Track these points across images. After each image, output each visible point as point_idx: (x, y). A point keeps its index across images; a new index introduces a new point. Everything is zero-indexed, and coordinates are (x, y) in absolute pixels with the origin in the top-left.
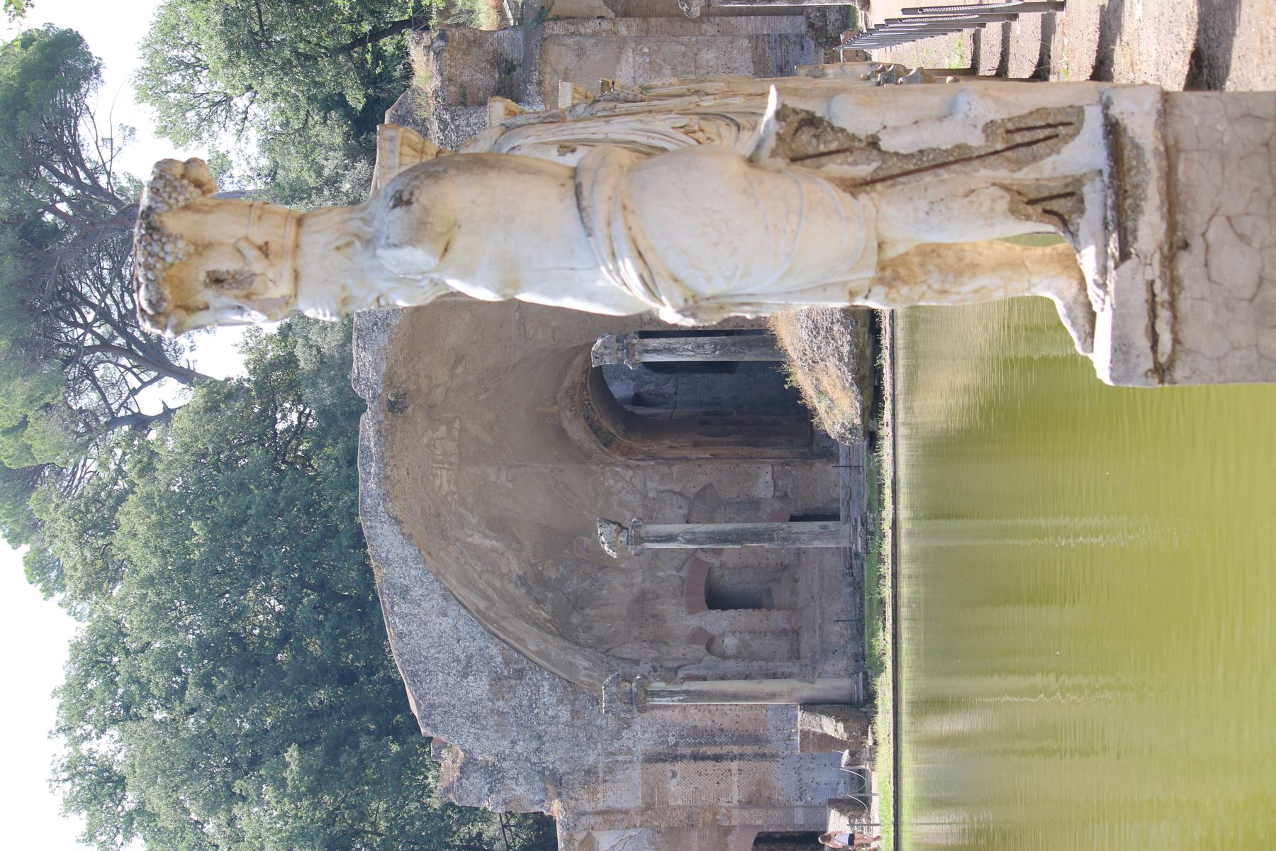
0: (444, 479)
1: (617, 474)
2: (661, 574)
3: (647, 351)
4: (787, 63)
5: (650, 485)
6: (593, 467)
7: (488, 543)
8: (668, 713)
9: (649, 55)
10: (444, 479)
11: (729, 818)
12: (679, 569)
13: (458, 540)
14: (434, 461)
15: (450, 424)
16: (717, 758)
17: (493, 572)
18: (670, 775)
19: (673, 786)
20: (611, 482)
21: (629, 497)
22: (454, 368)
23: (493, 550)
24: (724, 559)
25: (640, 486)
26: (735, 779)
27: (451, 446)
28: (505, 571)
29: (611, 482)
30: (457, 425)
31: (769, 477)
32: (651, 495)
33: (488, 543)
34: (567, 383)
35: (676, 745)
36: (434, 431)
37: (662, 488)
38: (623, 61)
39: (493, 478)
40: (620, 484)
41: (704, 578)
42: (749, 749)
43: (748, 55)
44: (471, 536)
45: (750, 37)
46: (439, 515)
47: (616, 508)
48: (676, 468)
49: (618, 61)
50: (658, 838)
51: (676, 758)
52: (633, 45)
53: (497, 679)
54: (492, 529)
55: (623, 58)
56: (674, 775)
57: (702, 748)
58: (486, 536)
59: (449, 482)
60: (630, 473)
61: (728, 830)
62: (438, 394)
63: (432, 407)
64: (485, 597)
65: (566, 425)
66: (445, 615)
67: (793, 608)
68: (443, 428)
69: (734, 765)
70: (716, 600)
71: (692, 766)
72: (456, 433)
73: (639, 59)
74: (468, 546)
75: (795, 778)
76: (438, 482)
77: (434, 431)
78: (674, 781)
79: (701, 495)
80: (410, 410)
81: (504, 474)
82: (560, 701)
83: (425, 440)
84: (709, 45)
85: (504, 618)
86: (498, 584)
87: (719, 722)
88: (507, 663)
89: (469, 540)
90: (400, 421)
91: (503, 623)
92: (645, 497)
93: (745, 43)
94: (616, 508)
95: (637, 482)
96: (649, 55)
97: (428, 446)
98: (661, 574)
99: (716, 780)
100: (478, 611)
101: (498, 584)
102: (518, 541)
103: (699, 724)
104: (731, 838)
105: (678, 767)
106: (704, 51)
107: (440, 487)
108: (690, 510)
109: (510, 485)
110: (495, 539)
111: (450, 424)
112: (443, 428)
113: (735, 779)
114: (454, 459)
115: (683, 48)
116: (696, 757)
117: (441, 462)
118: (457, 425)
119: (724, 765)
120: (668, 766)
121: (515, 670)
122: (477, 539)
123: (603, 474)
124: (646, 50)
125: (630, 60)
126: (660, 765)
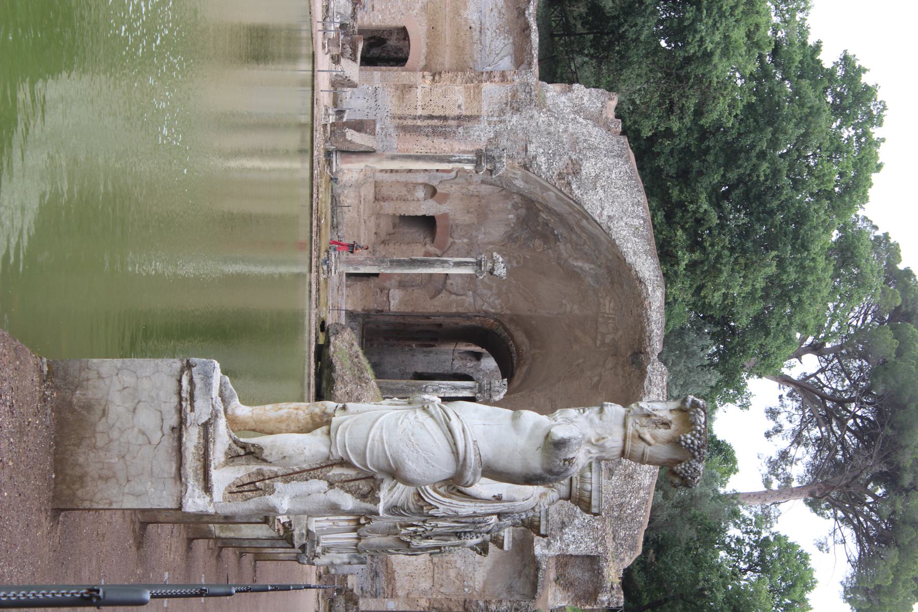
0: (607, 307)
1: (492, 308)
2: (465, 240)
3: (471, 388)
4: (372, 579)
5: (472, 300)
6: (509, 312)
7: (580, 264)
8: (462, 148)
9: (464, 586)
10: (607, 307)
11: (424, 77)
12: (453, 243)
13: (600, 266)
14: (614, 319)
15: (603, 343)
16: (431, 117)
17: (577, 244)
18: (463, 107)
19: (461, 100)
20: (497, 302)
21: (485, 291)
22: (599, 381)
23: (576, 259)
24: (423, 250)
25: (478, 298)
26: (419, 103)
27: (602, 329)
28: (569, 245)
29: (497, 302)
30: (598, 343)
31: (392, 302)
32: (471, 293)
33: (580, 264)
34: (524, 369)
35: (458, 126)
37: (464, 297)
38: (482, 583)
39: (575, 307)
40: (491, 300)
41: (437, 237)
42: (410, 122)
43: (398, 584)
44: (590, 269)
45: (397, 596)
46: (612, 283)
47: (494, 285)
48: (454, 310)
49: (485, 583)
50: (471, 65)
51: (459, 118)
52: (475, 593)
53: (576, 173)
54: (577, 273)
55: (481, 585)
56: (459, 106)
57: (441, 125)
58: (581, 268)
59: (604, 305)
60: (484, 308)
61: (425, 68)
62: (610, 363)
63: (615, 355)
64: (583, 229)
65: (526, 341)
66: (609, 217)
67: (378, 216)
68: (607, 341)
69: (419, 112)
70: (428, 223)
71: (447, 113)
72: (599, 337)
73: (471, 584)
74: (593, 263)
75: (379, 103)
76: (612, 305)
77: (614, 339)
78: (460, 102)
79: (439, 292)
80: (629, 353)
81: (568, 309)
82: (535, 158)
83: (620, 333)
84: (424, 592)
85: (570, 213)
86: (574, 237)
87: (430, 142)
88: (569, 184)
89: (592, 266)
90: (636, 346)
91: (571, 210)
92: (474, 292)
93: (401, 593)
94: (494, 285)
95: (480, 302)
96: (464, 586)
97: (617, 329)
98: (465, 240)
99: (432, 103)
100: (587, 219)
101: (574, 237)
102: (559, 264)
103: (442, 140)
104: (423, 63)
105: (457, 112)
106: (428, 588)
107: (610, 302)
108: (445, 282)
109: (564, 301)
110: (575, 266)
111: (603, 343)
112: (607, 341)
113: (419, 103)
114: (601, 320)
115: (442, 590)
116: (445, 118)
117: (610, 318)
118: (598, 343)
119: (426, 113)
120: (464, 113)
121: (564, 179)
122: (587, 266)
123: (502, 308)
124: (466, 590)
125: (477, 583)
126: (468, 113)
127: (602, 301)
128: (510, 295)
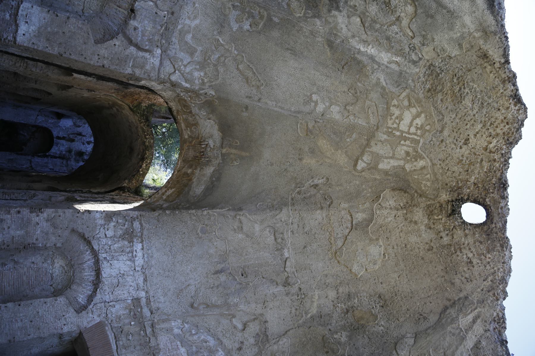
5: (157, 62)
7: (371, 50)
20: (196, 74)
21: (181, 55)
29: (196, 74)
32: (159, 51)
33: (371, 50)
36: (403, 168)
37: (147, 55)
40: (188, 70)
58: (372, 58)
74: (400, 53)
95: (168, 68)
109: (315, 97)
110: (359, 52)
111: (373, 167)
122: (384, 57)
123: (203, 83)
127: (396, 112)
128: (221, 70)
